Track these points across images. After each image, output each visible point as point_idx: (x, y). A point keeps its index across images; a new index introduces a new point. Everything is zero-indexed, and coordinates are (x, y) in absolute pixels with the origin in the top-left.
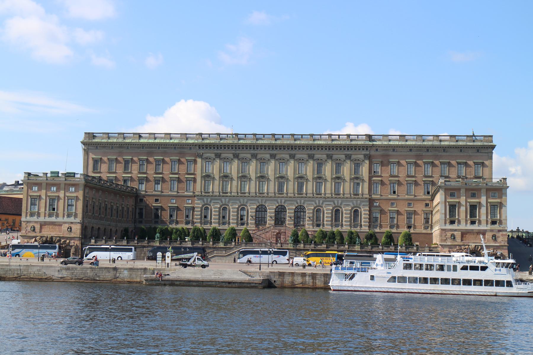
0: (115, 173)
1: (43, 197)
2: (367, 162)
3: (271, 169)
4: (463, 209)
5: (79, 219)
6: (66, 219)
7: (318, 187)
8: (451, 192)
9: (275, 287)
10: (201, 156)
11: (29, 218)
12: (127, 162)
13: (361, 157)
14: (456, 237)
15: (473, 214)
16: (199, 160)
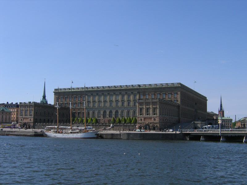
0: (63, 101)
1: (24, 110)
2: (138, 94)
3: (108, 98)
4: (144, 110)
5: (33, 117)
6: (29, 117)
7: (117, 104)
8: (141, 104)
9: (103, 138)
10: (87, 95)
11: (20, 117)
12: (66, 98)
13: (136, 92)
14: (142, 120)
15: (147, 111)
16: (86, 96)
